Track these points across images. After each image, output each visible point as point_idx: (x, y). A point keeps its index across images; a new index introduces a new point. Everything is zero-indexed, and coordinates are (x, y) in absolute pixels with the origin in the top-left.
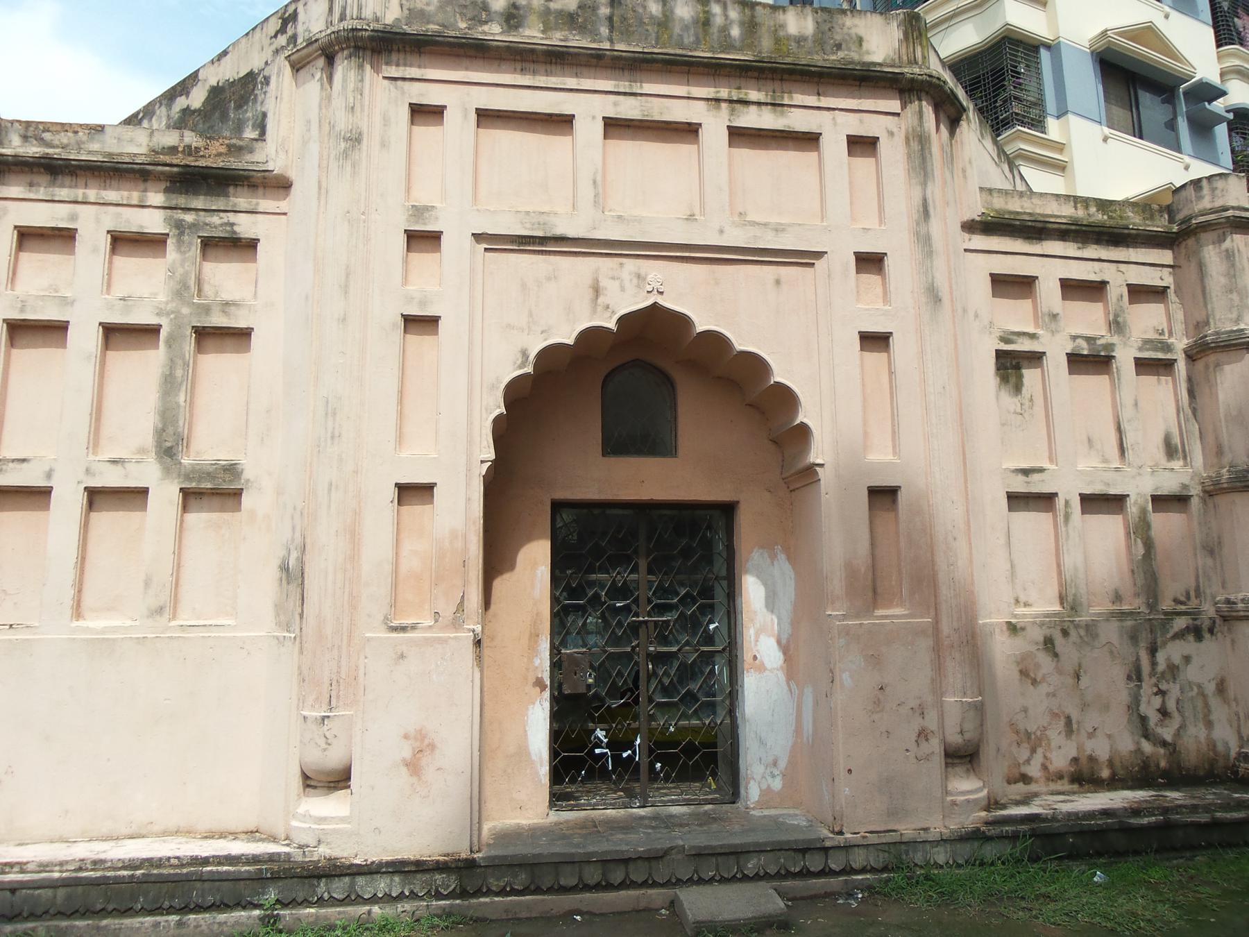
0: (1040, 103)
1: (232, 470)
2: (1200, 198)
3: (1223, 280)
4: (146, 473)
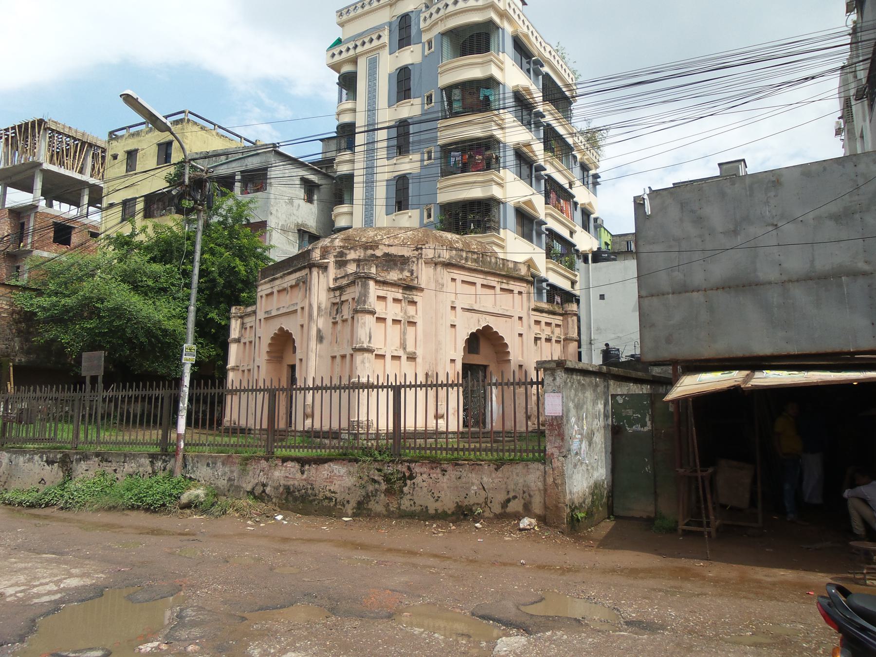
0: (499, 222)
1: (415, 353)
4: (400, 353)
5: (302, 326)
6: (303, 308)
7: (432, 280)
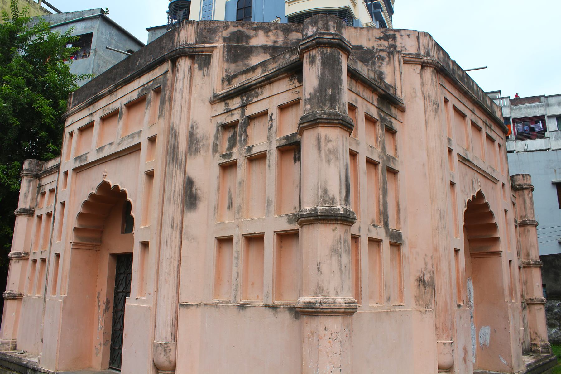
2: (524, 180)
3: (529, 205)
4: (380, 233)
5: (150, 175)
7: (419, 94)
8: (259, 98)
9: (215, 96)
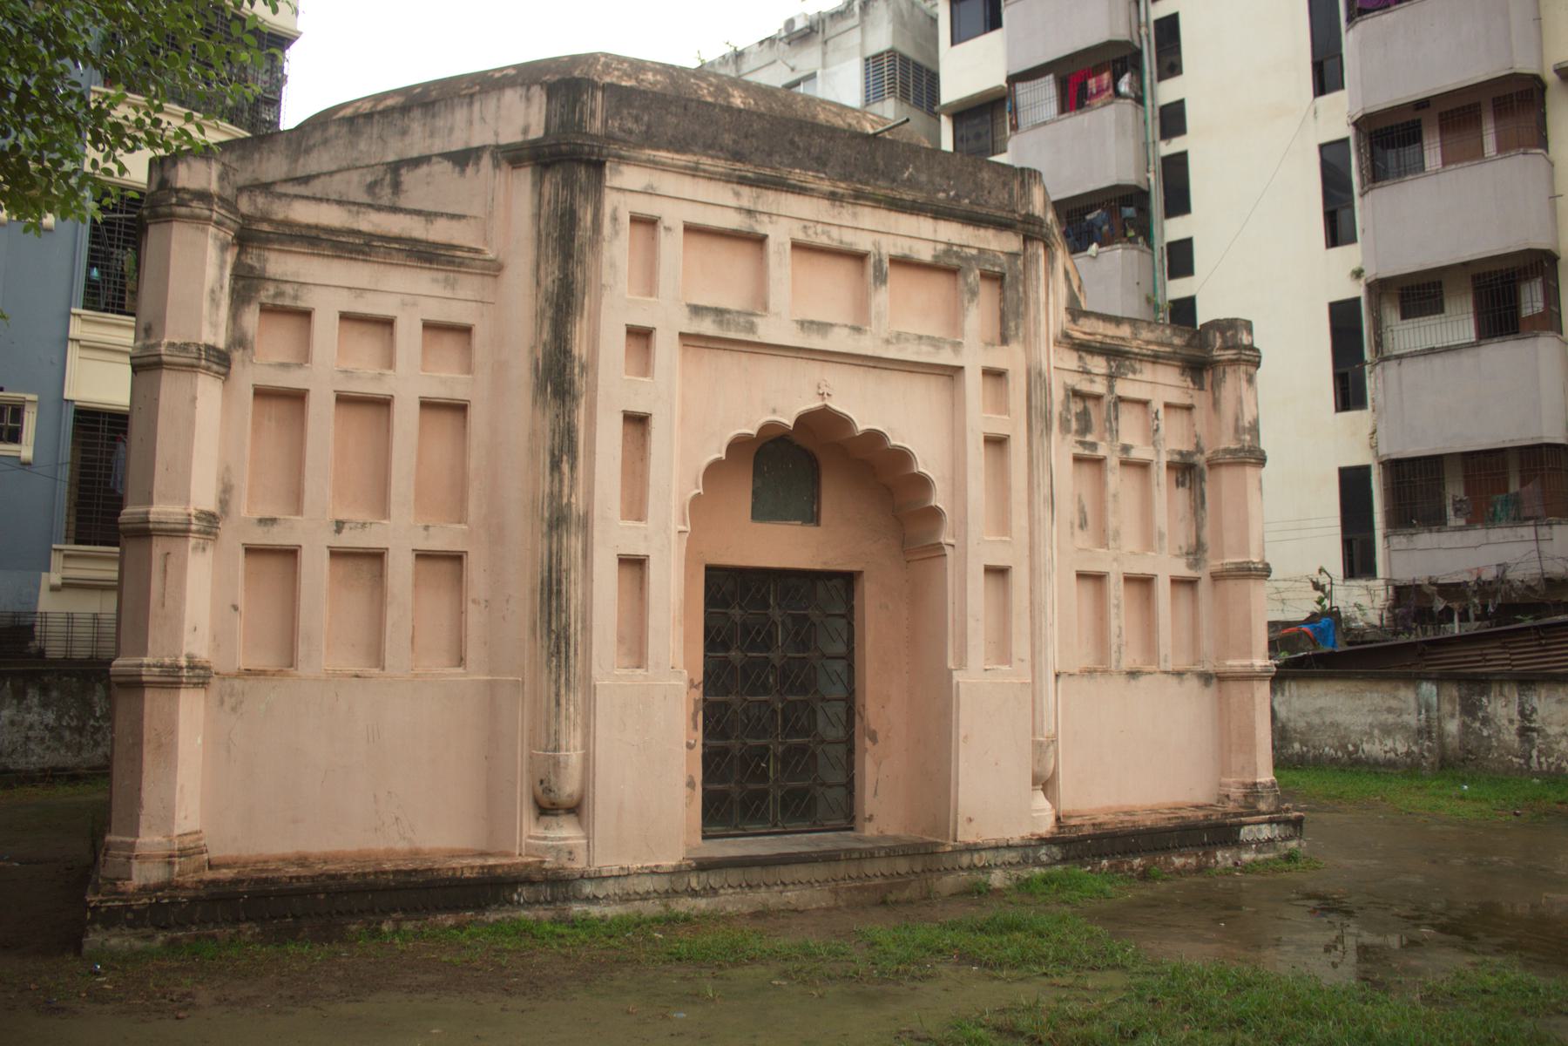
5: (996, 443)
6: (995, 375)
8: (1138, 377)
9: (1067, 336)
